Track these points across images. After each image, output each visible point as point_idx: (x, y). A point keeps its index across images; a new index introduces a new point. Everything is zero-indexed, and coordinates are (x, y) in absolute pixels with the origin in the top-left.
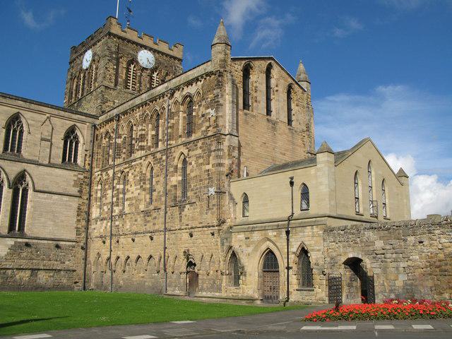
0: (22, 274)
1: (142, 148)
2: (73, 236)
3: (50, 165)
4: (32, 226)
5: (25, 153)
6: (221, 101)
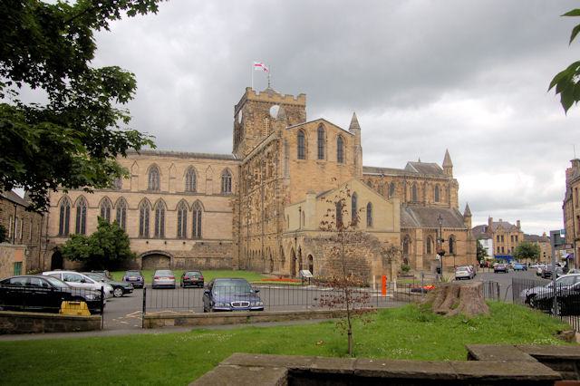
0: (200, 261)
1: (257, 183)
2: (230, 237)
3: (214, 195)
4: (206, 233)
5: (198, 191)
6: (279, 158)
